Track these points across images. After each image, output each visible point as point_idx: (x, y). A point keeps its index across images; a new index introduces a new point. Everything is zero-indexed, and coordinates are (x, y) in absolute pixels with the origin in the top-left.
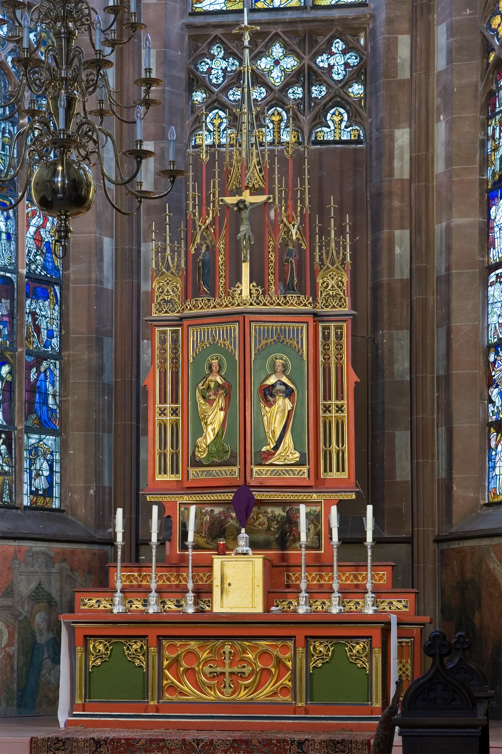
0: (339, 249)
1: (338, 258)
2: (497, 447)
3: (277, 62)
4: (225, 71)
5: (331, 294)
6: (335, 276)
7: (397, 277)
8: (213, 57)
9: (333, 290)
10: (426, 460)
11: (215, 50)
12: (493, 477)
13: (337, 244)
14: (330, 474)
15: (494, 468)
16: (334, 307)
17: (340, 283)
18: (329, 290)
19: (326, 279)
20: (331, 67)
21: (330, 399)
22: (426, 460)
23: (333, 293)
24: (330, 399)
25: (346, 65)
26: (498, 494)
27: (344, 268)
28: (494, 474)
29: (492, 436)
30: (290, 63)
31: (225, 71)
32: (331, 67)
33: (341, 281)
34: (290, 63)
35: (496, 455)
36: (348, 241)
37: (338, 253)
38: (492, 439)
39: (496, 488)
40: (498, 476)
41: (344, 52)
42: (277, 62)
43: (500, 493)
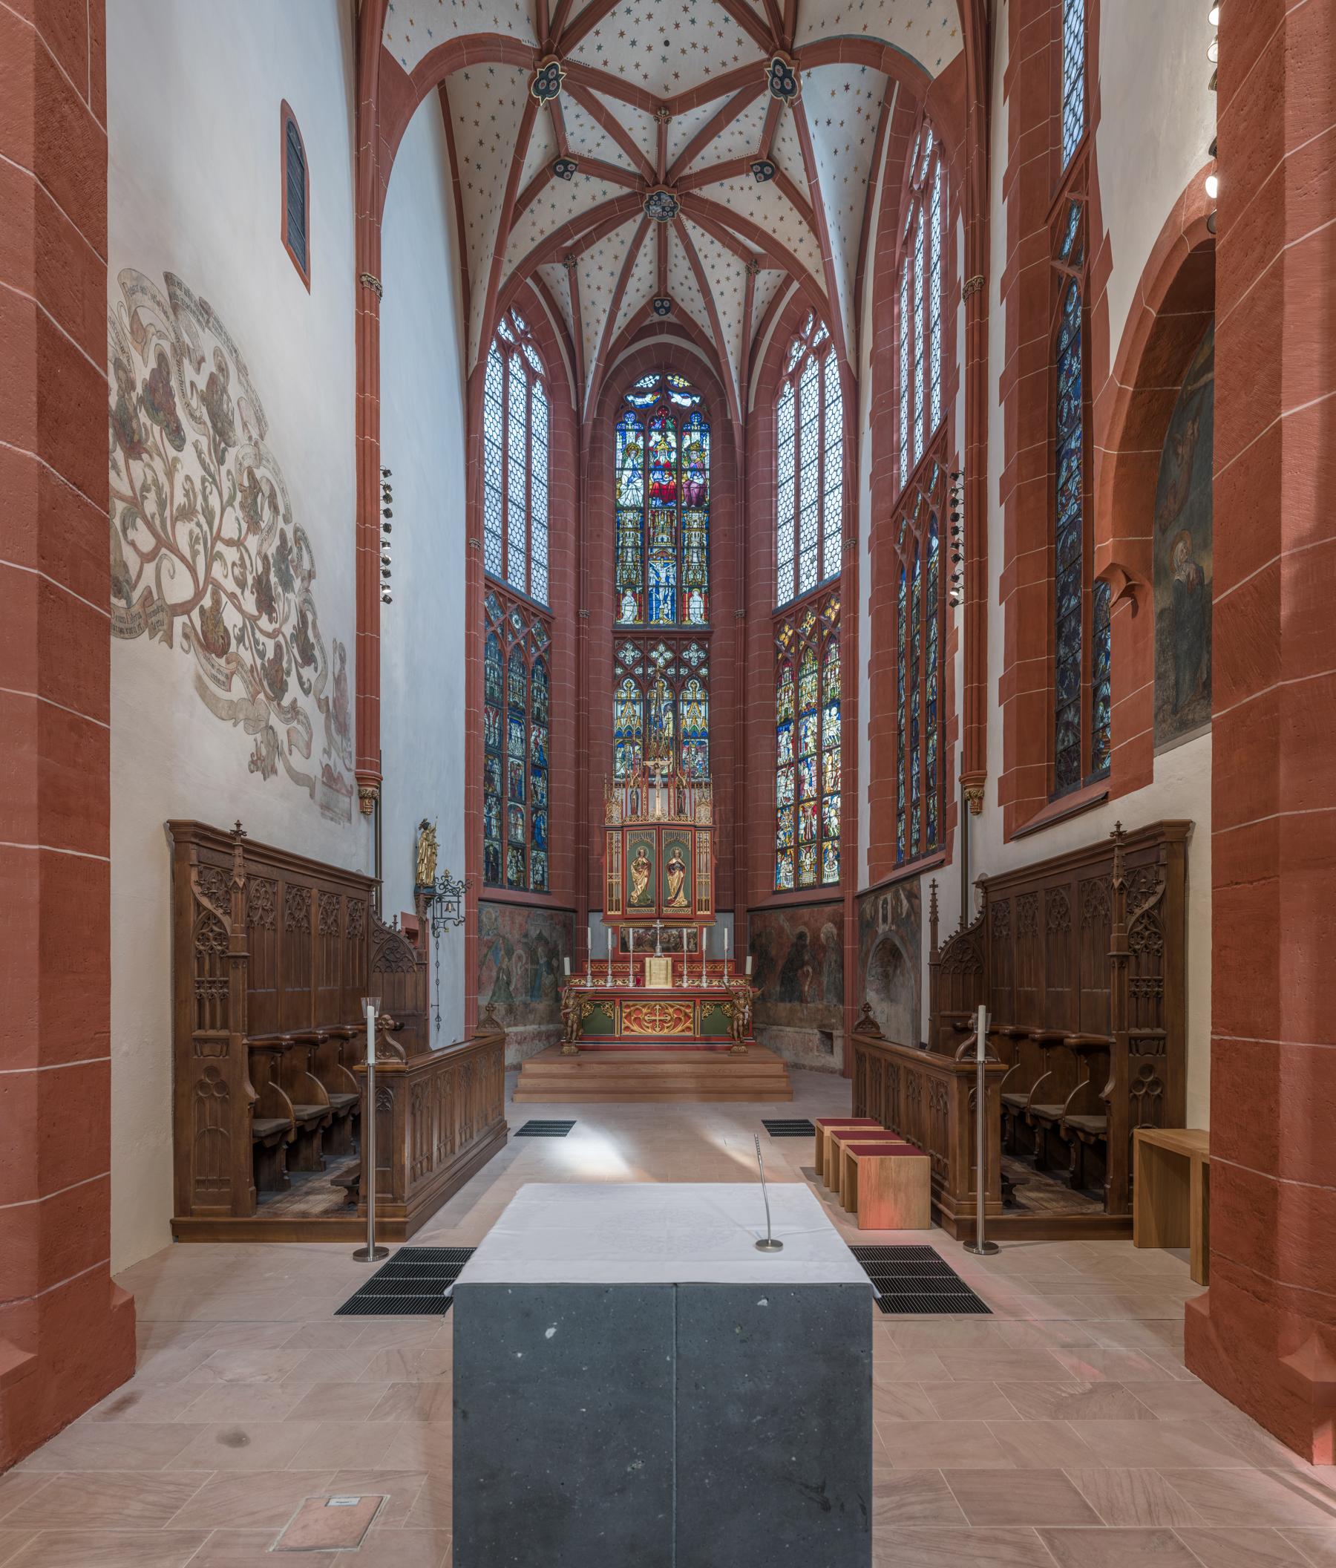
3: (661, 655)
4: (633, 657)
8: (626, 649)
11: (628, 646)
20: (690, 658)
25: (699, 657)
30: (668, 655)
31: (633, 657)
32: (690, 658)
34: (668, 655)
41: (697, 651)
42: (661, 655)
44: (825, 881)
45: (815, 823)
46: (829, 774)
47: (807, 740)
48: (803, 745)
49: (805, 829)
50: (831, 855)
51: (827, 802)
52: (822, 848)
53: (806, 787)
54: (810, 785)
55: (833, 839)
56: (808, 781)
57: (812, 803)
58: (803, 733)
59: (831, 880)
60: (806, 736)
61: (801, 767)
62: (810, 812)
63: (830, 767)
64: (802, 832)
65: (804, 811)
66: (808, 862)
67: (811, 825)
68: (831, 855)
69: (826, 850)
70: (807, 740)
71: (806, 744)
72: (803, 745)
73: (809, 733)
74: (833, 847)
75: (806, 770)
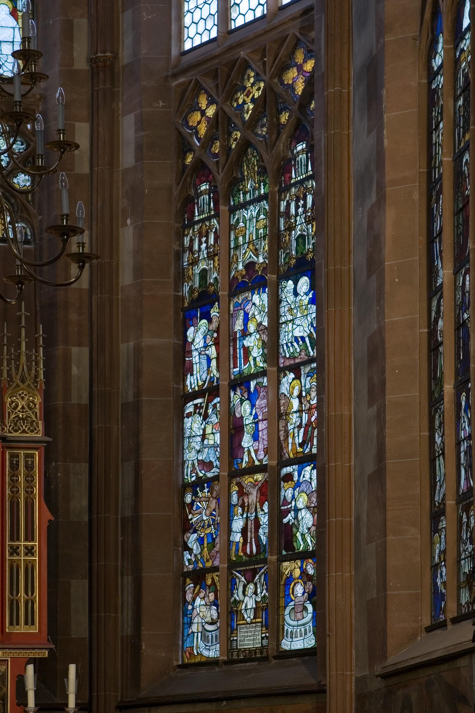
0: (31, 364)
1: (30, 374)
2: (194, 600)
5: (21, 416)
6: (26, 395)
7: (74, 400)
9: (23, 412)
10: (108, 614)
12: (188, 635)
13: (29, 358)
14: (17, 627)
15: (190, 624)
16: (24, 431)
17: (31, 404)
18: (19, 411)
19: (15, 398)
21: (18, 539)
22: (108, 614)
23: (23, 415)
24: (18, 539)
26: (196, 654)
27: (36, 387)
28: (190, 631)
29: (187, 588)
33: (33, 402)
35: (193, 609)
36: (42, 356)
37: (29, 369)
38: (188, 591)
39: (193, 647)
40: (196, 634)
43: (198, 653)
44: (286, 645)
45: (264, 520)
46: (294, 418)
47: (249, 342)
48: (240, 353)
49: (244, 531)
50: (299, 589)
51: (289, 477)
52: (279, 573)
53: (247, 441)
54: (255, 437)
55: (304, 556)
56: (248, 430)
57: (259, 477)
58: (238, 326)
59: (298, 644)
60: (245, 333)
61: (235, 398)
62: (253, 497)
63: (295, 404)
64: (237, 538)
65: (241, 493)
66: (250, 603)
67: (257, 525)
68: (299, 589)
69: (290, 579)
70: (249, 342)
71: (247, 351)
72: (240, 353)
73: (252, 327)
74: (304, 572)
75: (247, 406)
